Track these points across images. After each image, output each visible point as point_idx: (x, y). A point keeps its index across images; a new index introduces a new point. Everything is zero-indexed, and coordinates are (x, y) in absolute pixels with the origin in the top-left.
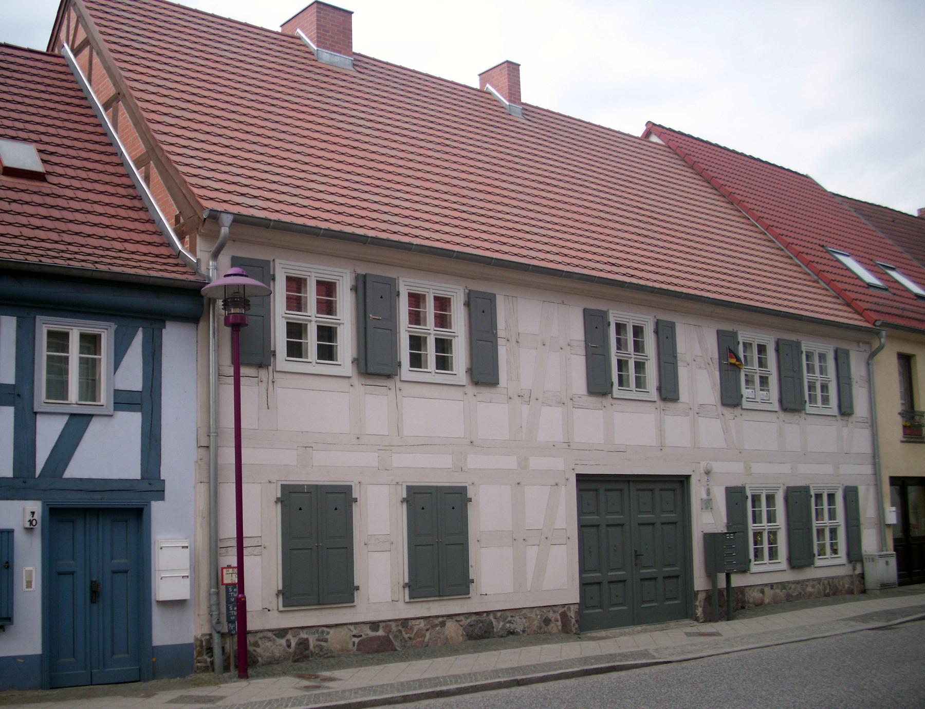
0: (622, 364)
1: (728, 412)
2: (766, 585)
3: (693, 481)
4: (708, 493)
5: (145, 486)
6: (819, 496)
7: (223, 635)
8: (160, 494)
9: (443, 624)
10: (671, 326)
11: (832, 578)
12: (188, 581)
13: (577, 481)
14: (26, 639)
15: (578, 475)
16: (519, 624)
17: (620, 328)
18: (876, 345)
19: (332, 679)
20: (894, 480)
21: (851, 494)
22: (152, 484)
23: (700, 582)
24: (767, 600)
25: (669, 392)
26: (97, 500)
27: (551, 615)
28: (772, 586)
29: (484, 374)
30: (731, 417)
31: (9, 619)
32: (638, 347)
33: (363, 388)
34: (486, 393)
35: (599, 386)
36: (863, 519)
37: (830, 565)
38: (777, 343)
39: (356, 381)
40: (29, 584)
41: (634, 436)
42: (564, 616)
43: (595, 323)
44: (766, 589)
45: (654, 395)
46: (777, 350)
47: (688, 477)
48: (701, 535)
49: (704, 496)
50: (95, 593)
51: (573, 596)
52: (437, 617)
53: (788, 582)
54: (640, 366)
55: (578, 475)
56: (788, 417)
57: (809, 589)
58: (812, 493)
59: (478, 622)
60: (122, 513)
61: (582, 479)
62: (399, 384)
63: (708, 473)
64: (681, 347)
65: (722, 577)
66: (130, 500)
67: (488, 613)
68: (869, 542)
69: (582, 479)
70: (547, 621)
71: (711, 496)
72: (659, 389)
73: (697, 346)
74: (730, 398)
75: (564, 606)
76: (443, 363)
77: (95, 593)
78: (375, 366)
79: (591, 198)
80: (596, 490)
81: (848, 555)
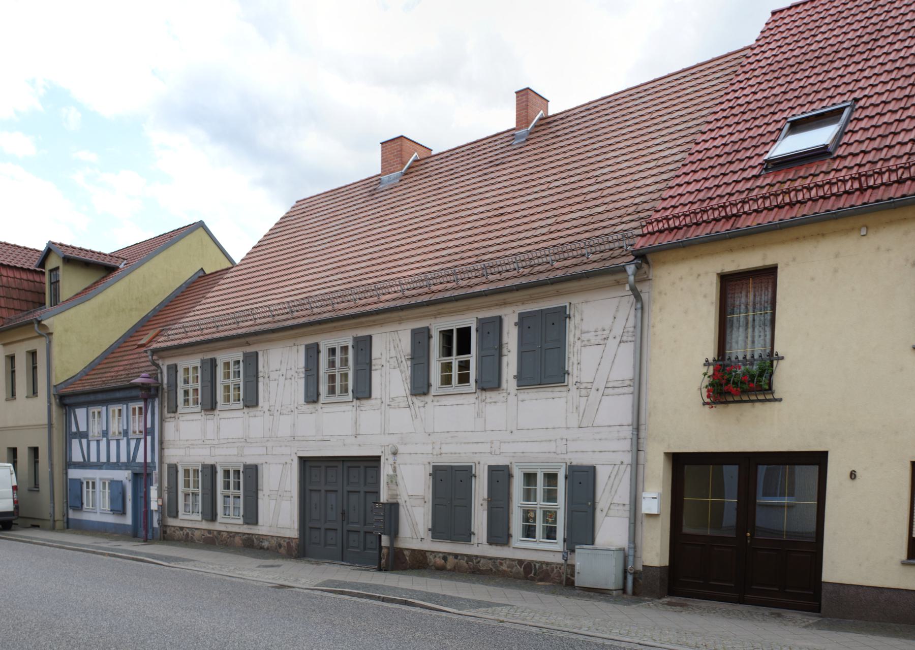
1: (418, 401)
2: (450, 554)
3: (382, 460)
4: (395, 470)
11: (547, 564)
24: (449, 567)
25: (363, 392)
28: (456, 556)
30: (422, 404)
34: (252, 411)
44: (450, 558)
49: (391, 472)
53: (477, 557)
57: (504, 567)
63: (395, 454)
69: (303, 461)
71: (398, 473)
79: (402, 248)
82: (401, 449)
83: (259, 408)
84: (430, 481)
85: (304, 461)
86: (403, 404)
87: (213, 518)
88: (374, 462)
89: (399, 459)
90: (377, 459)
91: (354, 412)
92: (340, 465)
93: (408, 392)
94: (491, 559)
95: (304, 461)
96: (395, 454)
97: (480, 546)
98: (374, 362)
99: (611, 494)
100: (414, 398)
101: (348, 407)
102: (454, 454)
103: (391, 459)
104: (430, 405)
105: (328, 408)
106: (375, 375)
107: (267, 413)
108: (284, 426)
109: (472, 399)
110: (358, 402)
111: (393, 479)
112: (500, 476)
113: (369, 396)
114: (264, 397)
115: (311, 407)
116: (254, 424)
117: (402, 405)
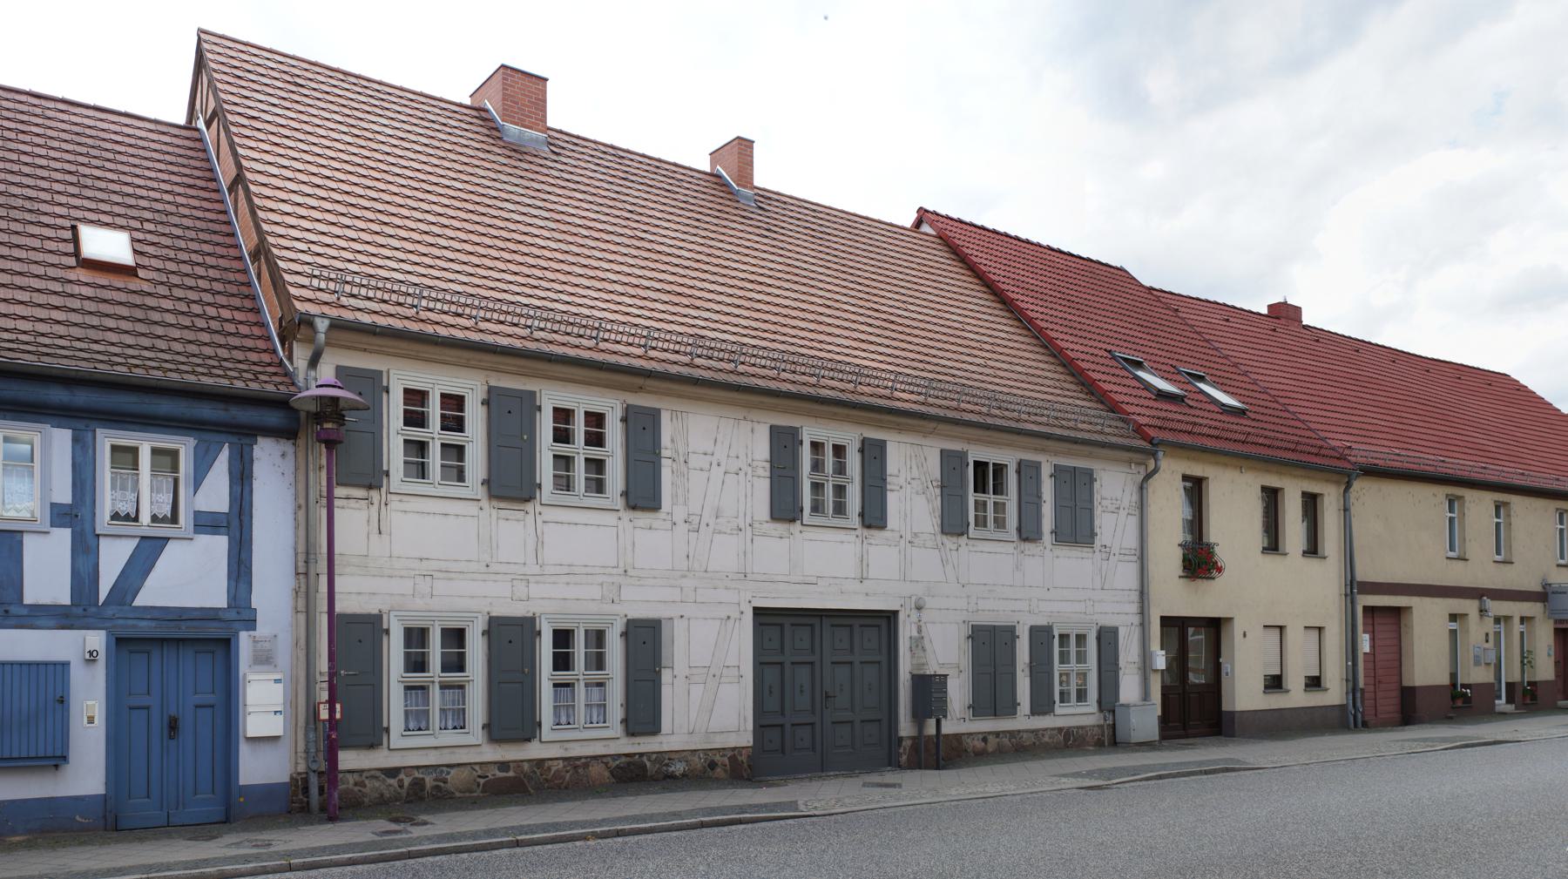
0: (817, 487)
1: (950, 542)
3: (901, 617)
4: (919, 631)
5: (232, 615)
6: (1064, 638)
7: (320, 774)
8: (251, 624)
9: (586, 765)
10: (882, 445)
12: (280, 718)
13: (755, 614)
14: (86, 774)
15: (755, 609)
16: (679, 768)
17: (816, 446)
18: (1152, 466)
19: (425, 823)
20: (1166, 621)
21: (1108, 638)
22: (241, 612)
23: (906, 728)
25: (873, 518)
26: (185, 631)
27: (717, 758)
29: (643, 495)
31: (65, 758)
32: (840, 469)
33: (494, 512)
34: (643, 518)
35: (785, 509)
36: (1122, 663)
37: (1081, 714)
38: (1020, 463)
39: (485, 503)
40: (91, 720)
41: (827, 567)
42: (733, 759)
43: (784, 443)
45: (855, 521)
46: (1019, 472)
47: (895, 613)
48: (908, 677)
49: (915, 633)
50: (173, 726)
51: (746, 739)
52: (579, 758)
54: (840, 490)
55: (755, 609)
56: (1028, 546)
58: (1056, 634)
59: (629, 764)
60: (208, 641)
61: (759, 612)
62: (539, 508)
63: (919, 608)
64: (891, 468)
65: (932, 722)
66: (213, 630)
67: (641, 755)
68: (1129, 689)
69: (759, 612)
70: (712, 765)
72: (862, 515)
73: (912, 466)
74: (953, 525)
75: (734, 749)
76: (598, 486)
77: (173, 726)
78: (511, 485)
80: (781, 625)
81: (1099, 702)
82: (929, 602)
83: (662, 514)
84: (967, 646)
85: (764, 617)
86: (929, 544)
87: (527, 730)
88: (889, 618)
89: (925, 615)
90: (890, 618)
91: (859, 541)
92: (816, 621)
93: (938, 529)
94: (1032, 731)
95: (764, 617)
96: (919, 608)
97: (1023, 721)
98: (889, 479)
99: (1129, 653)
100: (945, 539)
101: (851, 537)
102: (994, 612)
103: (914, 615)
104: (964, 549)
105: (811, 534)
106: (889, 494)
107: (682, 528)
108: (724, 554)
109: (1009, 548)
110: (866, 532)
111: (918, 643)
112: (1041, 636)
113: (883, 527)
114: (675, 496)
115: (781, 527)
116: (650, 540)
117: (929, 544)
